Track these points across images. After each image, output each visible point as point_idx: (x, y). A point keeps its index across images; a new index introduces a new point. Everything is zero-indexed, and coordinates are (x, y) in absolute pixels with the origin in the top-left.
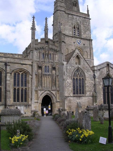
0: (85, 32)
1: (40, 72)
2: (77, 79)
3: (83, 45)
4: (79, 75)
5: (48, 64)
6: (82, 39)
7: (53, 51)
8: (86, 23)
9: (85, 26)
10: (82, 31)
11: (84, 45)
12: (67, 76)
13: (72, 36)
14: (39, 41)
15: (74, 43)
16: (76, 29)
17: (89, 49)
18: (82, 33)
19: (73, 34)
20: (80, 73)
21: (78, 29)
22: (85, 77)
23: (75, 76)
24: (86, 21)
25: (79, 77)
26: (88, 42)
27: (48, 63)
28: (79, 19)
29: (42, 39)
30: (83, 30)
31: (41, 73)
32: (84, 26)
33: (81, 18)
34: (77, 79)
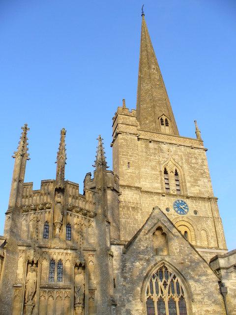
0: (196, 180)
1: (31, 281)
2: (161, 301)
3: (193, 214)
4: (168, 287)
5: (59, 253)
6: (188, 198)
7: (78, 217)
8: (196, 158)
9: (194, 168)
10: (188, 178)
11: (196, 212)
12: (124, 292)
13: (160, 191)
14: (37, 187)
15: (167, 210)
16: (171, 175)
17: (210, 222)
18: (188, 185)
19: (162, 188)
20: (169, 280)
21: (176, 174)
22: (188, 292)
23: (152, 293)
24: (195, 154)
25: (169, 293)
26: (207, 204)
27: (62, 251)
28: (176, 151)
29: (44, 183)
30: (191, 177)
31: (36, 283)
32: (192, 168)
33: (183, 148)
34: (161, 301)
